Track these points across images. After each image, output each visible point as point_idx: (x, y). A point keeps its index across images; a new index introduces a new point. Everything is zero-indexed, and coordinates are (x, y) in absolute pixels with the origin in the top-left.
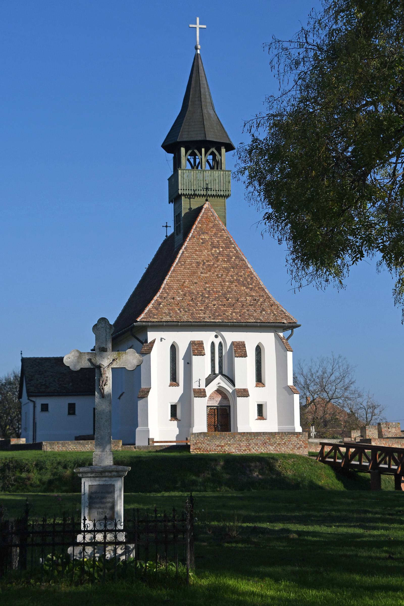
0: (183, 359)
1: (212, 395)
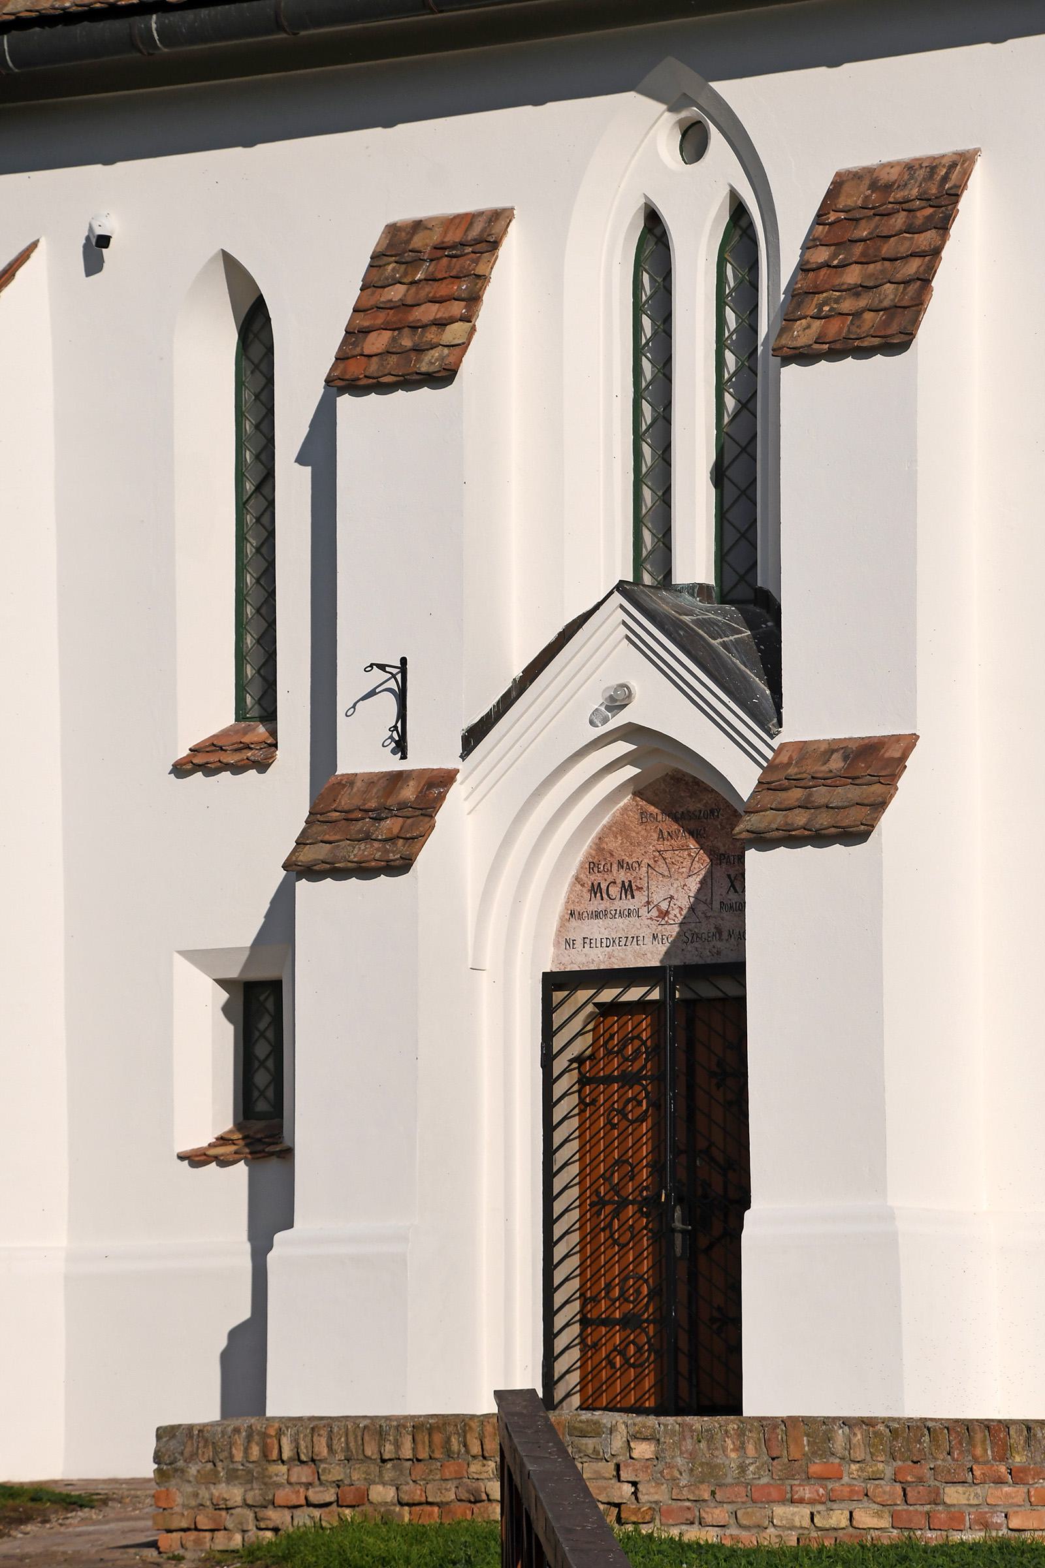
0: (301, 460)
1: (612, 844)
